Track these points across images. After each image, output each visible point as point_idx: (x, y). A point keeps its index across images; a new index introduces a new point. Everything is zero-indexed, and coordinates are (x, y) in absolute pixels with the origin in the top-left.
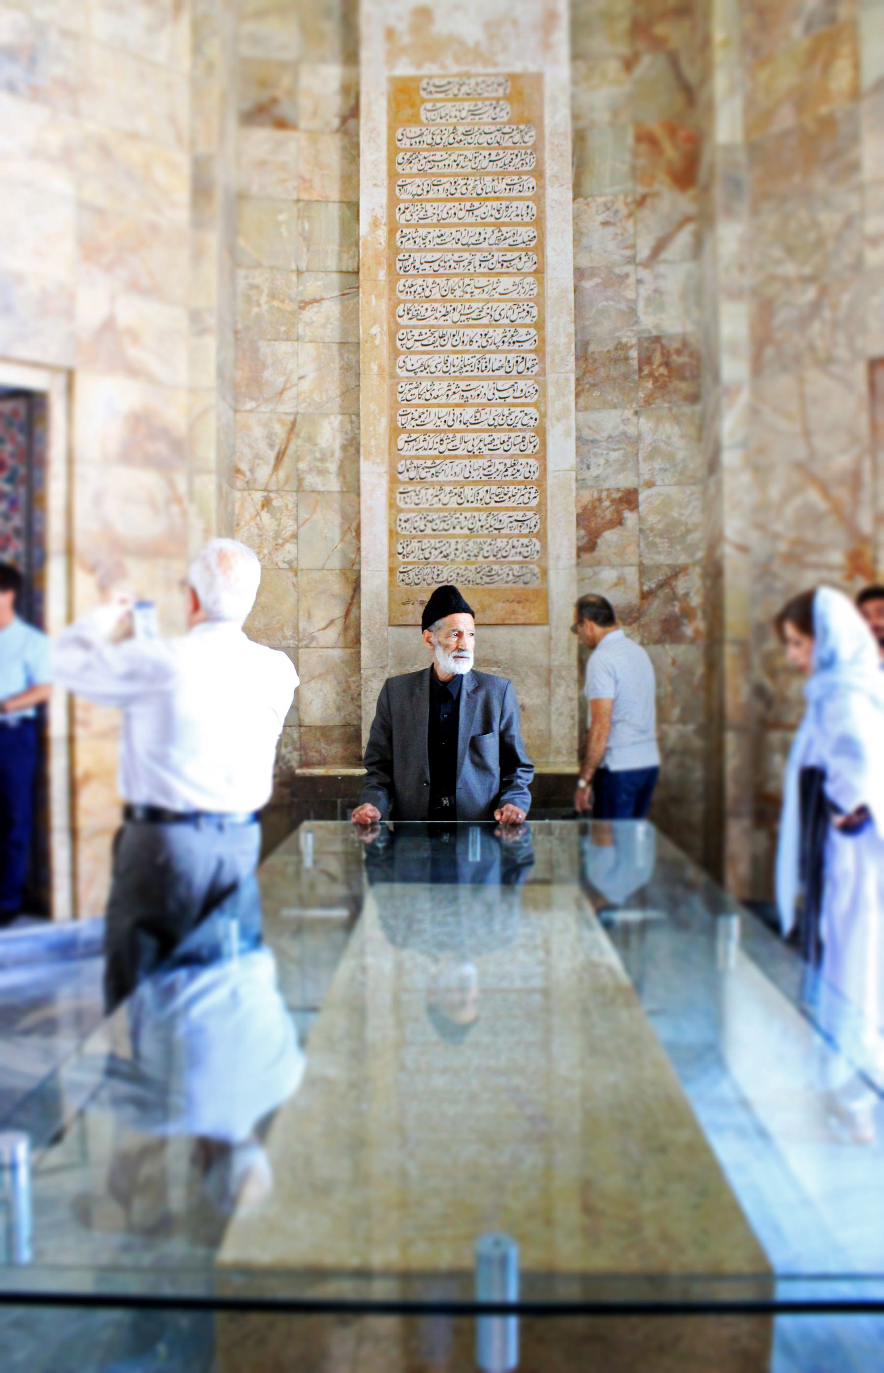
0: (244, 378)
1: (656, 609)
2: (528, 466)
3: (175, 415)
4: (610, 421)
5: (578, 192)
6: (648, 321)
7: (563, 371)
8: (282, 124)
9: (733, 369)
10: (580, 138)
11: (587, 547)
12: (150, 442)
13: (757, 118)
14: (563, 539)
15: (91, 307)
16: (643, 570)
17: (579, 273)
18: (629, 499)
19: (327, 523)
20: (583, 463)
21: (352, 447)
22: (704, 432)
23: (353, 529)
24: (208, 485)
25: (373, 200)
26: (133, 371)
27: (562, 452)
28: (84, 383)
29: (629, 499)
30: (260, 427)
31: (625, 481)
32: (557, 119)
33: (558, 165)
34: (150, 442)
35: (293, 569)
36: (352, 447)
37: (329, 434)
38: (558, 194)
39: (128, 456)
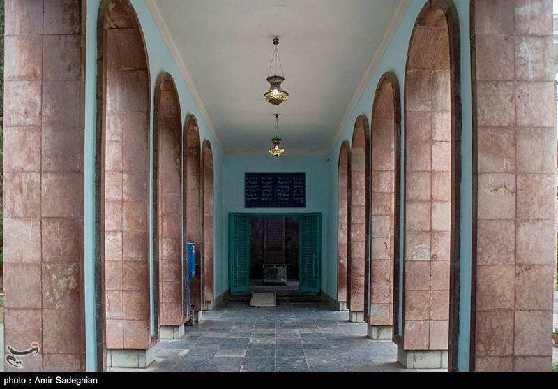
4: (289, 231)
7: (284, 226)
11: (287, 241)
14: (284, 243)
21: (263, 233)
23: (264, 241)
29: (290, 239)
36: (263, 233)
37: (261, 232)
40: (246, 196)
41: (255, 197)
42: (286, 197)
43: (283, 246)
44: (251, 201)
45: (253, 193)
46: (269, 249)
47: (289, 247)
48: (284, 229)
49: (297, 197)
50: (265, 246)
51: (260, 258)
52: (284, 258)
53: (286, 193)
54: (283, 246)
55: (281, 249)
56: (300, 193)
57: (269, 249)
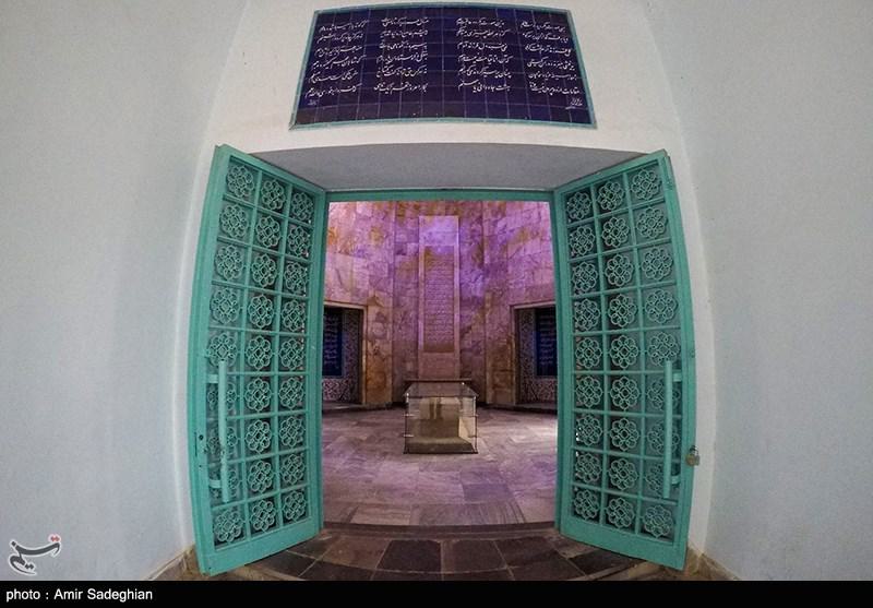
0: (397, 305)
1: (475, 348)
2: (451, 322)
3: (385, 312)
5: (460, 268)
6: (473, 293)
8: (404, 254)
9: (488, 305)
10: (460, 257)
11: (462, 337)
12: (381, 318)
13: (492, 260)
14: (457, 335)
15: (371, 293)
16: (473, 341)
17: (461, 284)
18: (470, 328)
19: (411, 332)
20: (461, 320)
22: (484, 316)
24: (390, 326)
25: (421, 270)
26: (378, 305)
27: (457, 318)
28: (370, 308)
29: (470, 328)
30: (399, 313)
31: (469, 324)
32: (457, 255)
33: (457, 263)
34: (381, 318)
35: (405, 340)
36: (417, 318)
37: (412, 314)
38: (457, 270)
39: (377, 321)
40: (306, 86)
41: (346, 84)
42: (501, 82)
43: (457, 344)
44: (326, 100)
45: (337, 70)
46: (429, 349)
47: (468, 343)
48: (457, 308)
49: (552, 83)
50: (421, 343)
51: (409, 366)
52: (458, 364)
53: (495, 66)
54: (457, 344)
55: (450, 349)
56: (557, 71)
57: (429, 349)
